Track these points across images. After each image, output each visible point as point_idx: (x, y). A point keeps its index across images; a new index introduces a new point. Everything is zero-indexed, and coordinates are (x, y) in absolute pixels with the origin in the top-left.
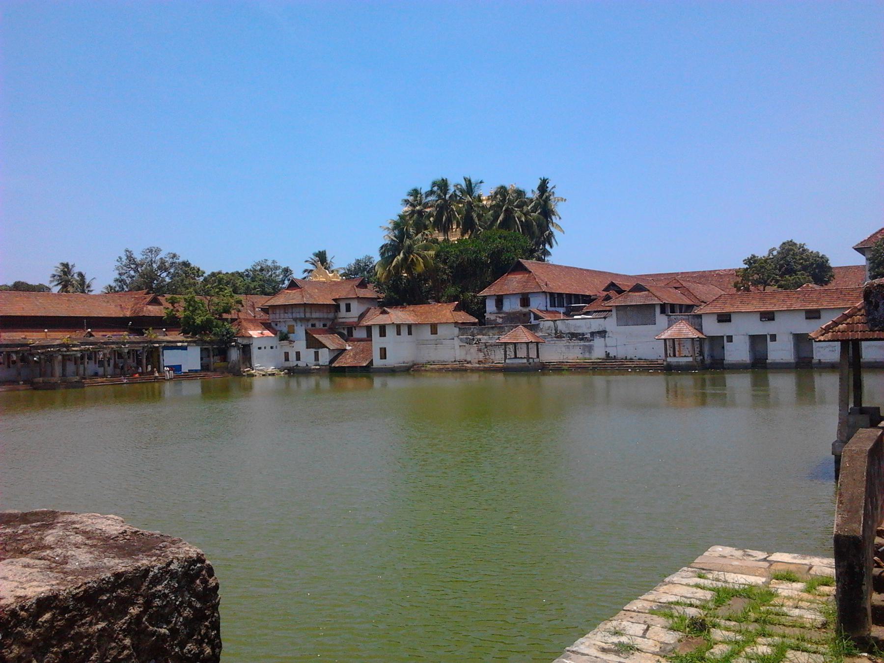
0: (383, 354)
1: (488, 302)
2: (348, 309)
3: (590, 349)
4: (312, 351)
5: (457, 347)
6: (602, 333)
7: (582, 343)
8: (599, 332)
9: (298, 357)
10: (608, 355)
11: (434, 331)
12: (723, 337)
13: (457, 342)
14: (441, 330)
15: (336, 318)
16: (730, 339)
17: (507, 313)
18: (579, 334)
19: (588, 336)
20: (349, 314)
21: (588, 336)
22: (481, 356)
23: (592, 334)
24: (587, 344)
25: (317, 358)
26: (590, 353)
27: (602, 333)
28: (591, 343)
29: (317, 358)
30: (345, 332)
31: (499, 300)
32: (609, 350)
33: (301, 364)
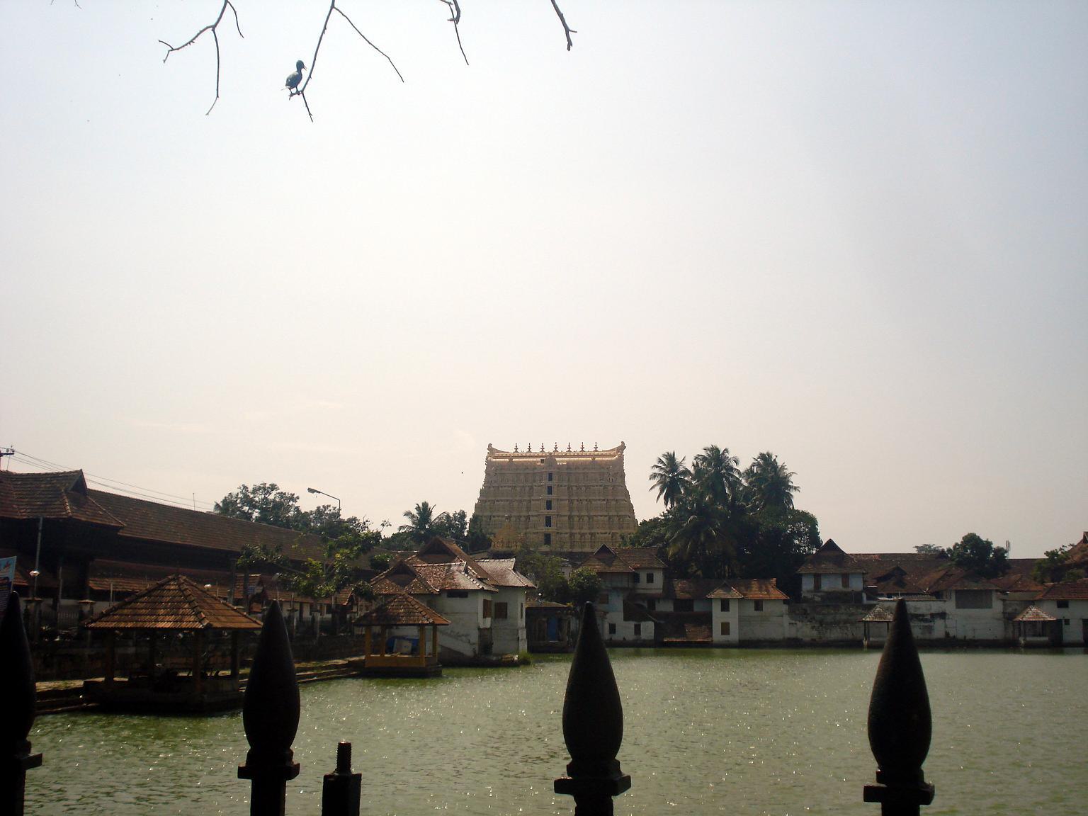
0: (725, 628)
1: (804, 580)
2: (650, 579)
3: (930, 629)
4: (632, 624)
5: (786, 624)
6: (943, 615)
7: (923, 624)
8: (938, 614)
9: (613, 629)
10: (947, 634)
11: (758, 605)
12: (1061, 620)
14: (767, 608)
16: (1067, 622)
17: (824, 592)
18: (920, 615)
19: (929, 617)
20: (650, 585)
21: (929, 617)
22: (815, 634)
23: (933, 615)
24: (927, 624)
25: (637, 630)
26: (930, 633)
28: (932, 624)
29: (637, 630)
30: (646, 605)
31: (817, 577)
32: (948, 630)
33: (618, 636)
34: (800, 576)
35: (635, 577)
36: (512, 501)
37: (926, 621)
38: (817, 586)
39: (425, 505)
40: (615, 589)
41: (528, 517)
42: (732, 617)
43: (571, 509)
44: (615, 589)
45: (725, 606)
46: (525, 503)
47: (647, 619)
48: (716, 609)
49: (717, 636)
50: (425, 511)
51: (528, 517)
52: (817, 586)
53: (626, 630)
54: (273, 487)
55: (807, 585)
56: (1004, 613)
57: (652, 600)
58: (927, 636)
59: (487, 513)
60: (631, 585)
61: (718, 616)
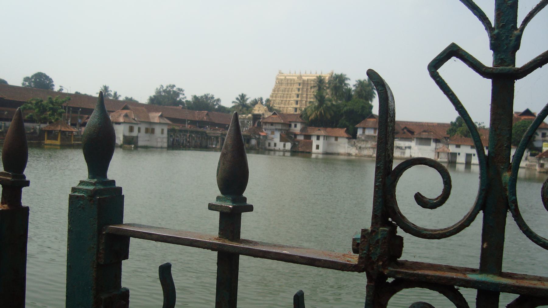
0: (318, 147)
2: (295, 126)
3: (404, 153)
4: (282, 143)
6: (410, 148)
7: (401, 151)
9: (275, 145)
13: (347, 145)
15: (289, 130)
16: (459, 154)
21: (404, 148)
23: (406, 147)
25: (284, 146)
27: (410, 148)
29: (284, 146)
30: (293, 136)
33: (277, 148)
34: (357, 128)
35: (290, 126)
36: (284, 94)
37: (403, 149)
38: (364, 132)
39: (243, 94)
40: (276, 129)
41: (289, 101)
42: (321, 142)
43: (307, 98)
44: (276, 129)
45: (318, 138)
46: (289, 95)
47: (288, 142)
48: (314, 139)
49: (314, 149)
50: (243, 97)
51: (289, 101)
52: (364, 132)
53: (280, 145)
54: (174, 86)
55: (360, 132)
56: (436, 149)
57: (296, 135)
58: (403, 156)
59: (274, 99)
60: (287, 129)
61: (315, 142)
